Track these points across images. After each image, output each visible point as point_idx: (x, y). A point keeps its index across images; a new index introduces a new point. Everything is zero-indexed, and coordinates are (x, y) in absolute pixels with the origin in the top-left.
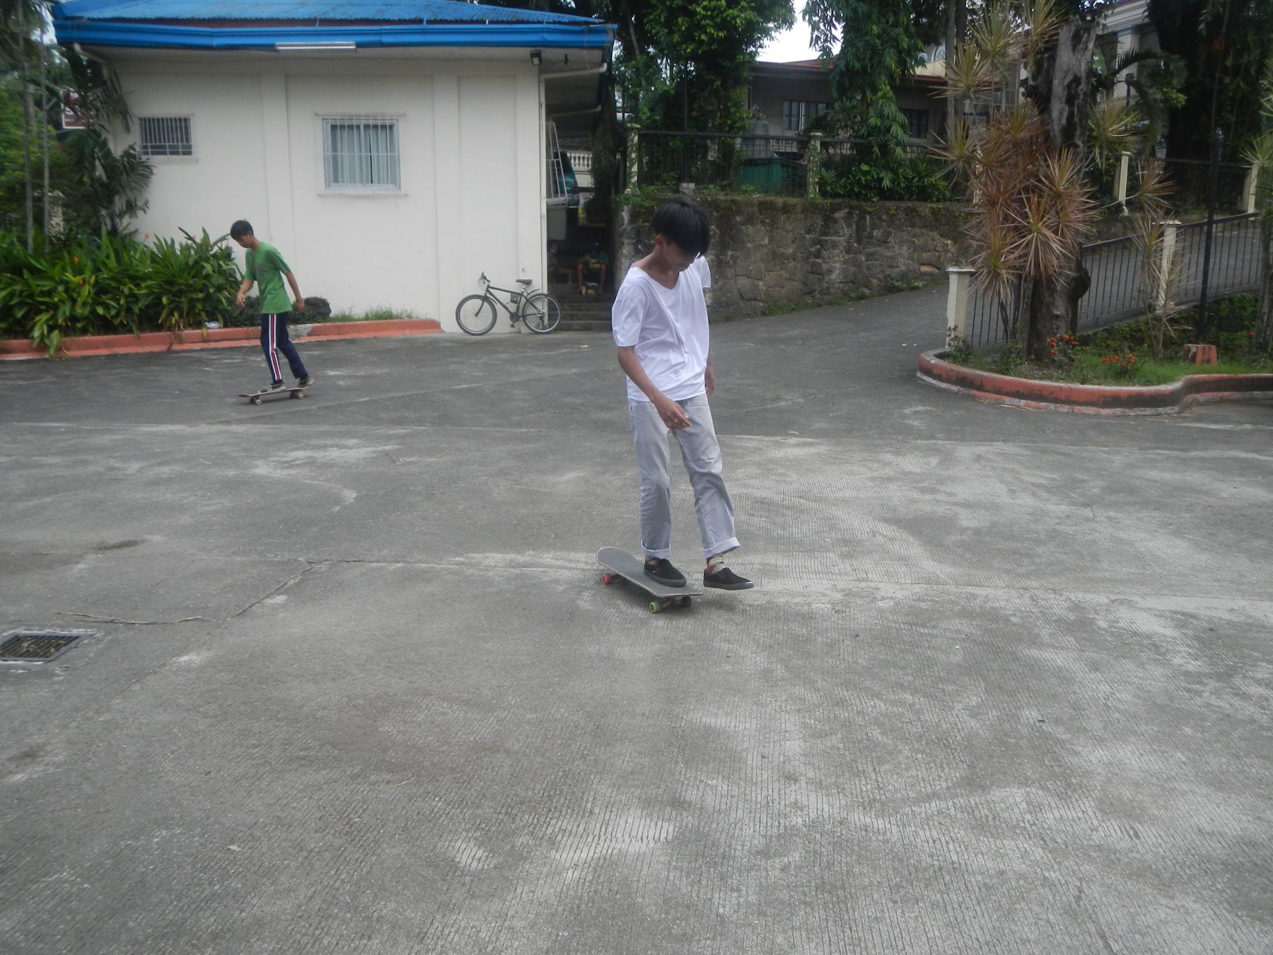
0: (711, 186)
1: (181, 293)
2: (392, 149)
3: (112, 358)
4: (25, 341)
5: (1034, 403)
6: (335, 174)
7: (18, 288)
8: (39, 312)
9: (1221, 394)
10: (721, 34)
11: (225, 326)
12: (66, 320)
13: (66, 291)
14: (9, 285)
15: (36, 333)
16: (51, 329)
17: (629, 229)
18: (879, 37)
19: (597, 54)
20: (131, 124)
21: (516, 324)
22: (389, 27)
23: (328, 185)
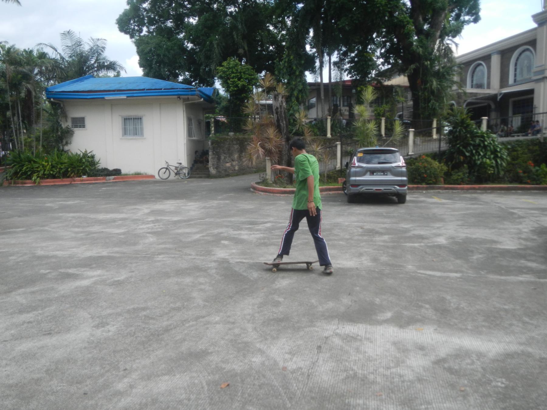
0: (238, 133)
1: (75, 167)
2: (141, 125)
3: (55, 185)
4: (31, 181)
5: (265, 193)
6: (125, 132)
7: (29, 166)
8: (35, 173)
9: (338, 192)
10: (235, 89)
11: (88, 177)
15: (33, 179)
16: (38, 177)
17: (211, 147)
18: (295, 85)
19: (196, 97)
21: (176, 176)
23: (123, 136)
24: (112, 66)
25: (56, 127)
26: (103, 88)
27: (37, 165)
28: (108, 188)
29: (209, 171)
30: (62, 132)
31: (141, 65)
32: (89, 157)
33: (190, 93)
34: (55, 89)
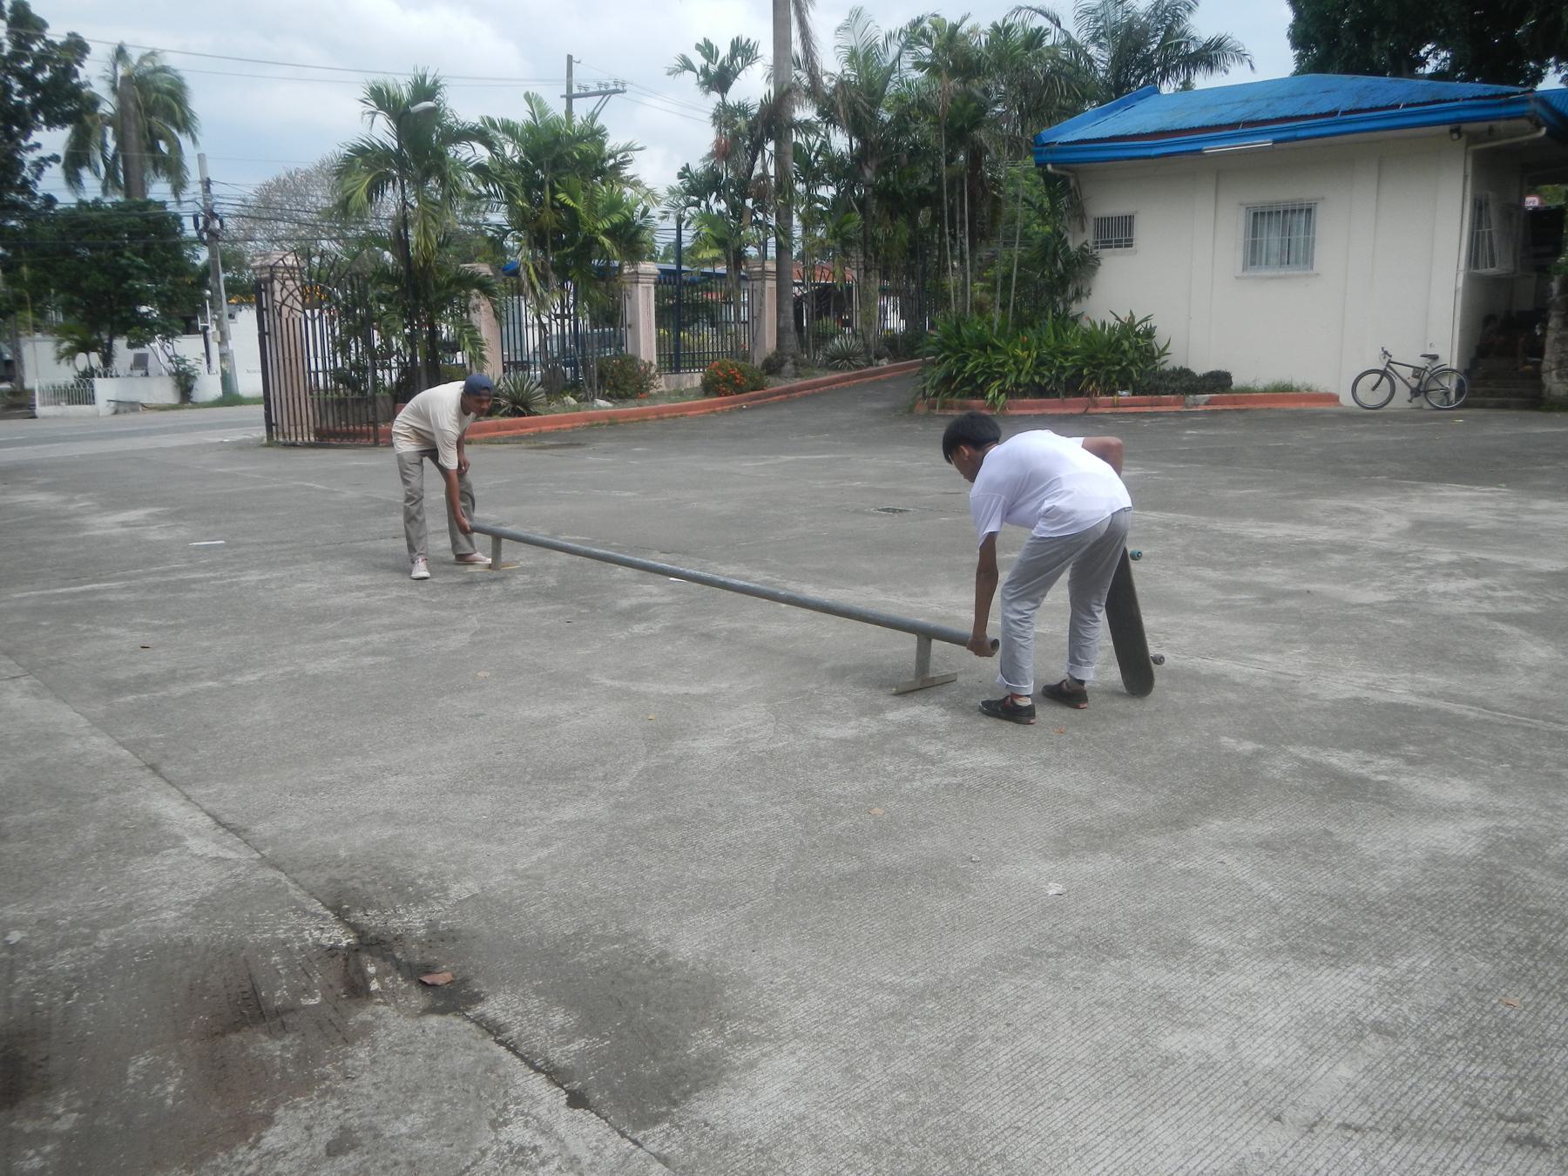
1: (1100, 366)
2: (1307, 232)
4: (981, 401)
6: (1254, 256)
7: (981, 360)
8: (994, 380)
11: (1133, 395)
12: (1011, 386)
13: (1014, 364)
14: (976, 358)
15: (990, 396)
16: (1000, 392)
17: (1558, 300)
19: (1524, 123)
20: (1086, 226)
21: (1415, 400)
22: (1303, 122)
24: (1210, 55)
25: (1051, 249)
26: (1196, 122)
27: (1001, 358)
28: (1202, 432)
29: (1541, 386)
30: (1067, 263)
31: (1300, 38)
32: (1137, 335)
33: (1504, 110)
34: (1057, 134)
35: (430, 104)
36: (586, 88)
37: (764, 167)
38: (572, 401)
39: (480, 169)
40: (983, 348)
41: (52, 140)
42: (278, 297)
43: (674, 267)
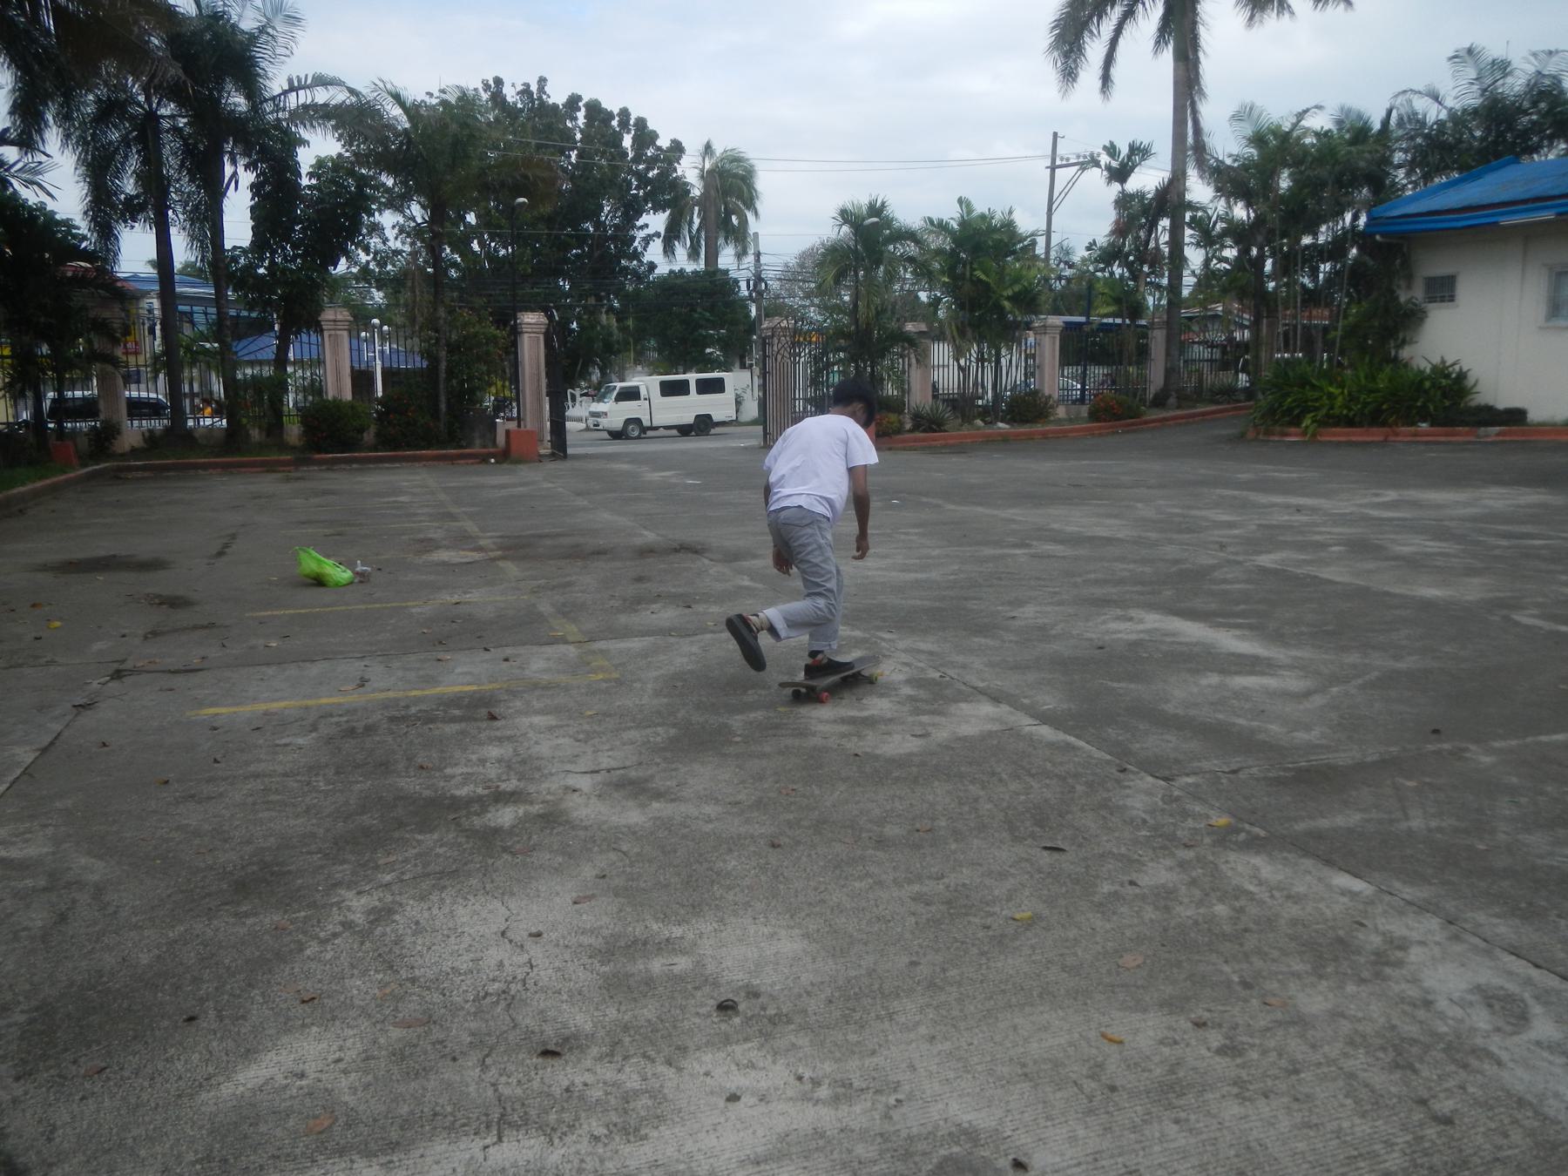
8: (1309, 412)
11: (1432, 426)
27: (1317, 394)
32: (1448, 376)
35: (875, 219)
36: (1068, 159)
37: (1157, 240)
38: (979, 422)
39: (911, 260)
40: (1302, 386)
41: (655, 221)
42: (775, 348)
43: (1083, 319)
